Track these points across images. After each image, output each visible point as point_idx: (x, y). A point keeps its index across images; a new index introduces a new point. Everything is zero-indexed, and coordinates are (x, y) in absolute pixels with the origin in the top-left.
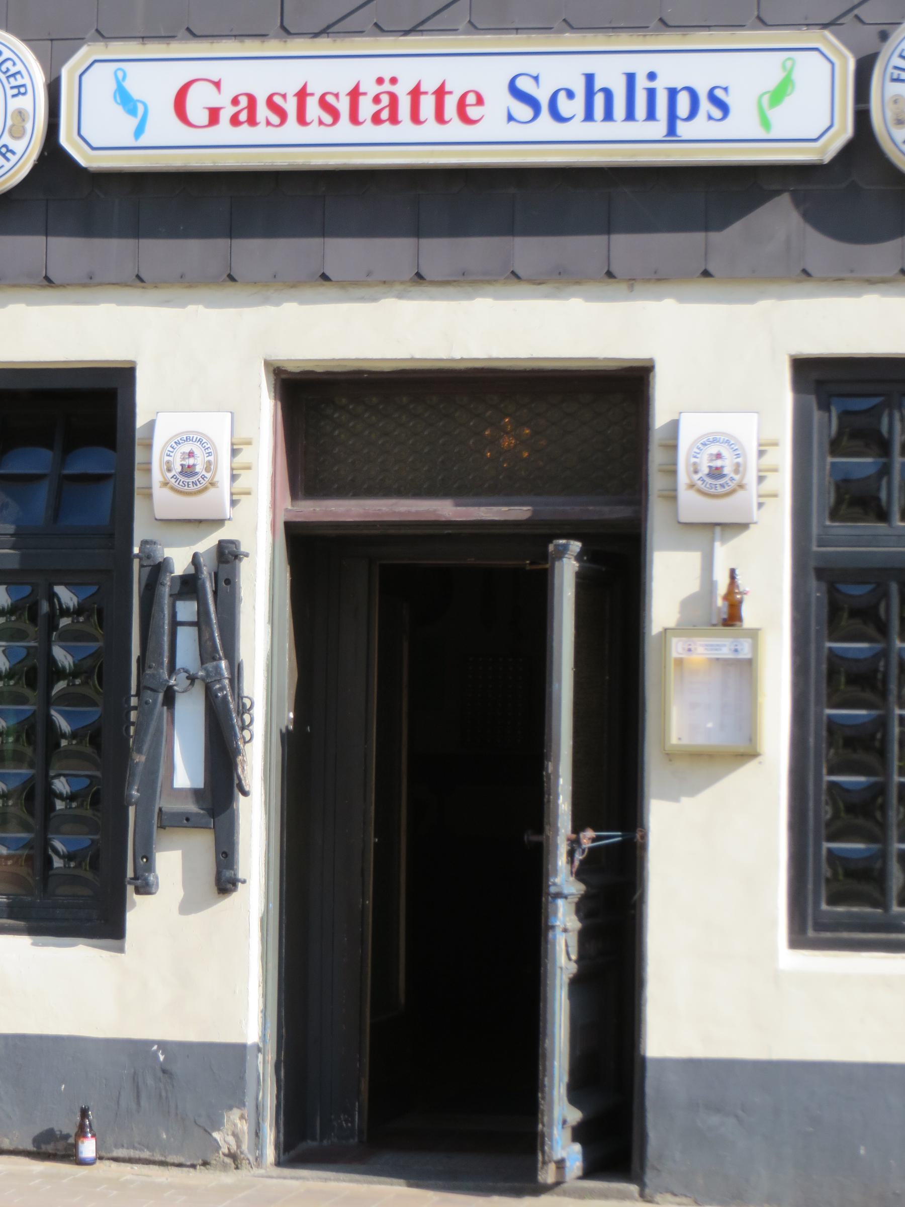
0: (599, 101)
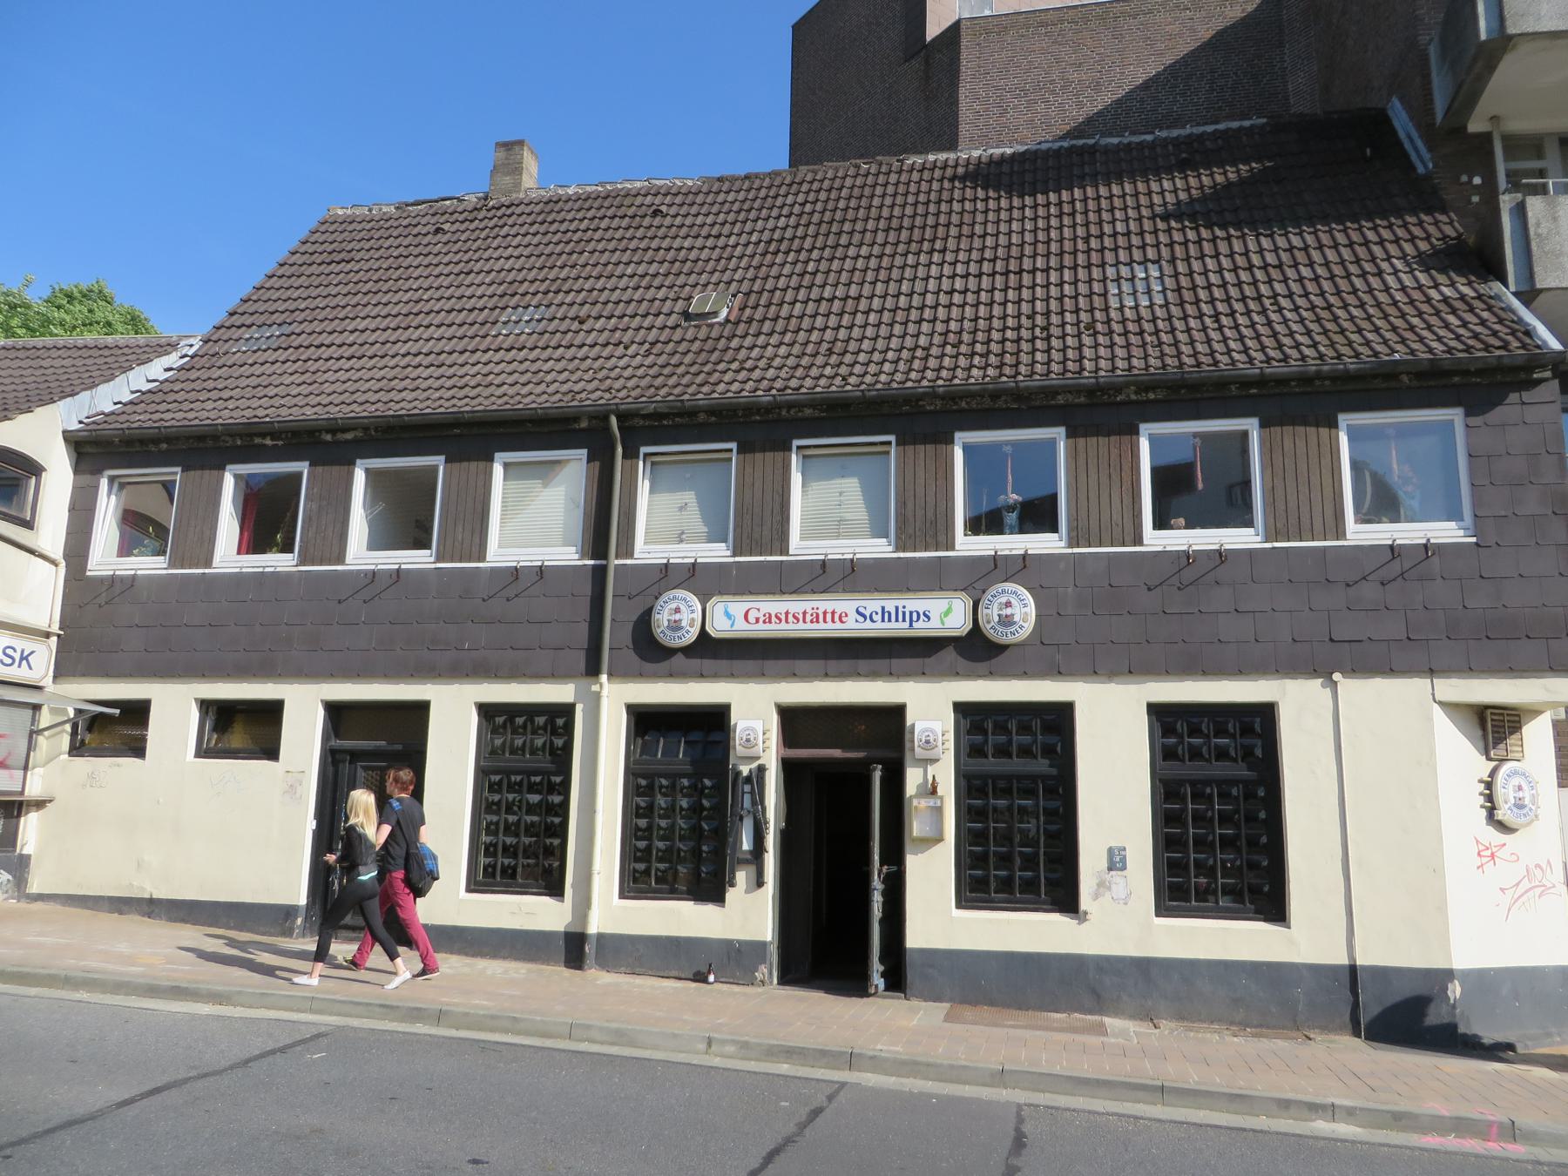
0: (886, 615)
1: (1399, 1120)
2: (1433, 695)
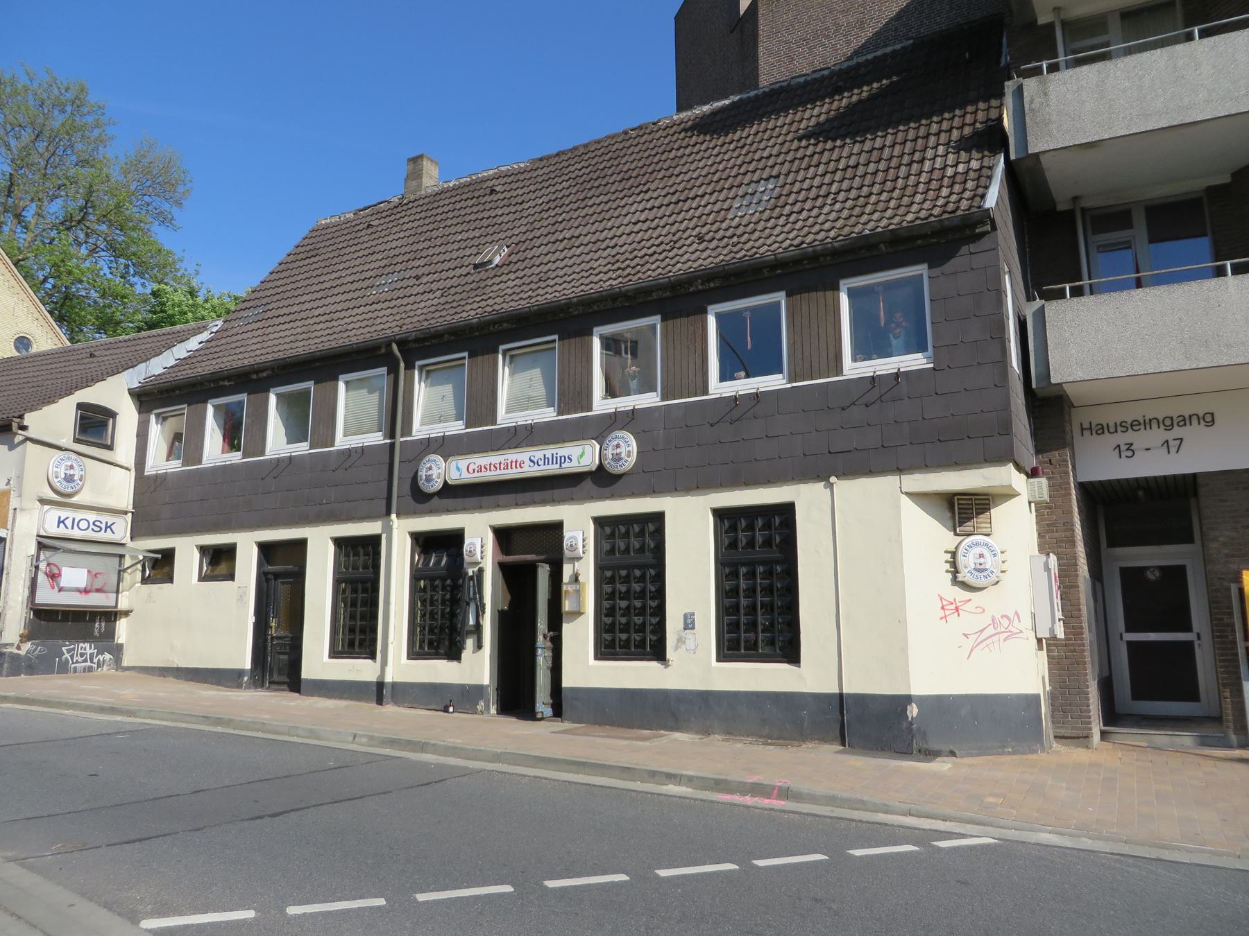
1: (720, 785)
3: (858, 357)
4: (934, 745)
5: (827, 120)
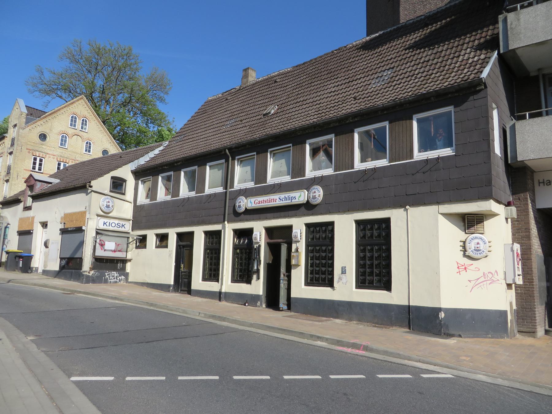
1: (339, 343)
2: (438, 211)
3: (421, 150)
4: (451, 332)
5: (419, 40)
